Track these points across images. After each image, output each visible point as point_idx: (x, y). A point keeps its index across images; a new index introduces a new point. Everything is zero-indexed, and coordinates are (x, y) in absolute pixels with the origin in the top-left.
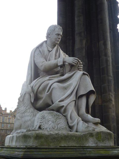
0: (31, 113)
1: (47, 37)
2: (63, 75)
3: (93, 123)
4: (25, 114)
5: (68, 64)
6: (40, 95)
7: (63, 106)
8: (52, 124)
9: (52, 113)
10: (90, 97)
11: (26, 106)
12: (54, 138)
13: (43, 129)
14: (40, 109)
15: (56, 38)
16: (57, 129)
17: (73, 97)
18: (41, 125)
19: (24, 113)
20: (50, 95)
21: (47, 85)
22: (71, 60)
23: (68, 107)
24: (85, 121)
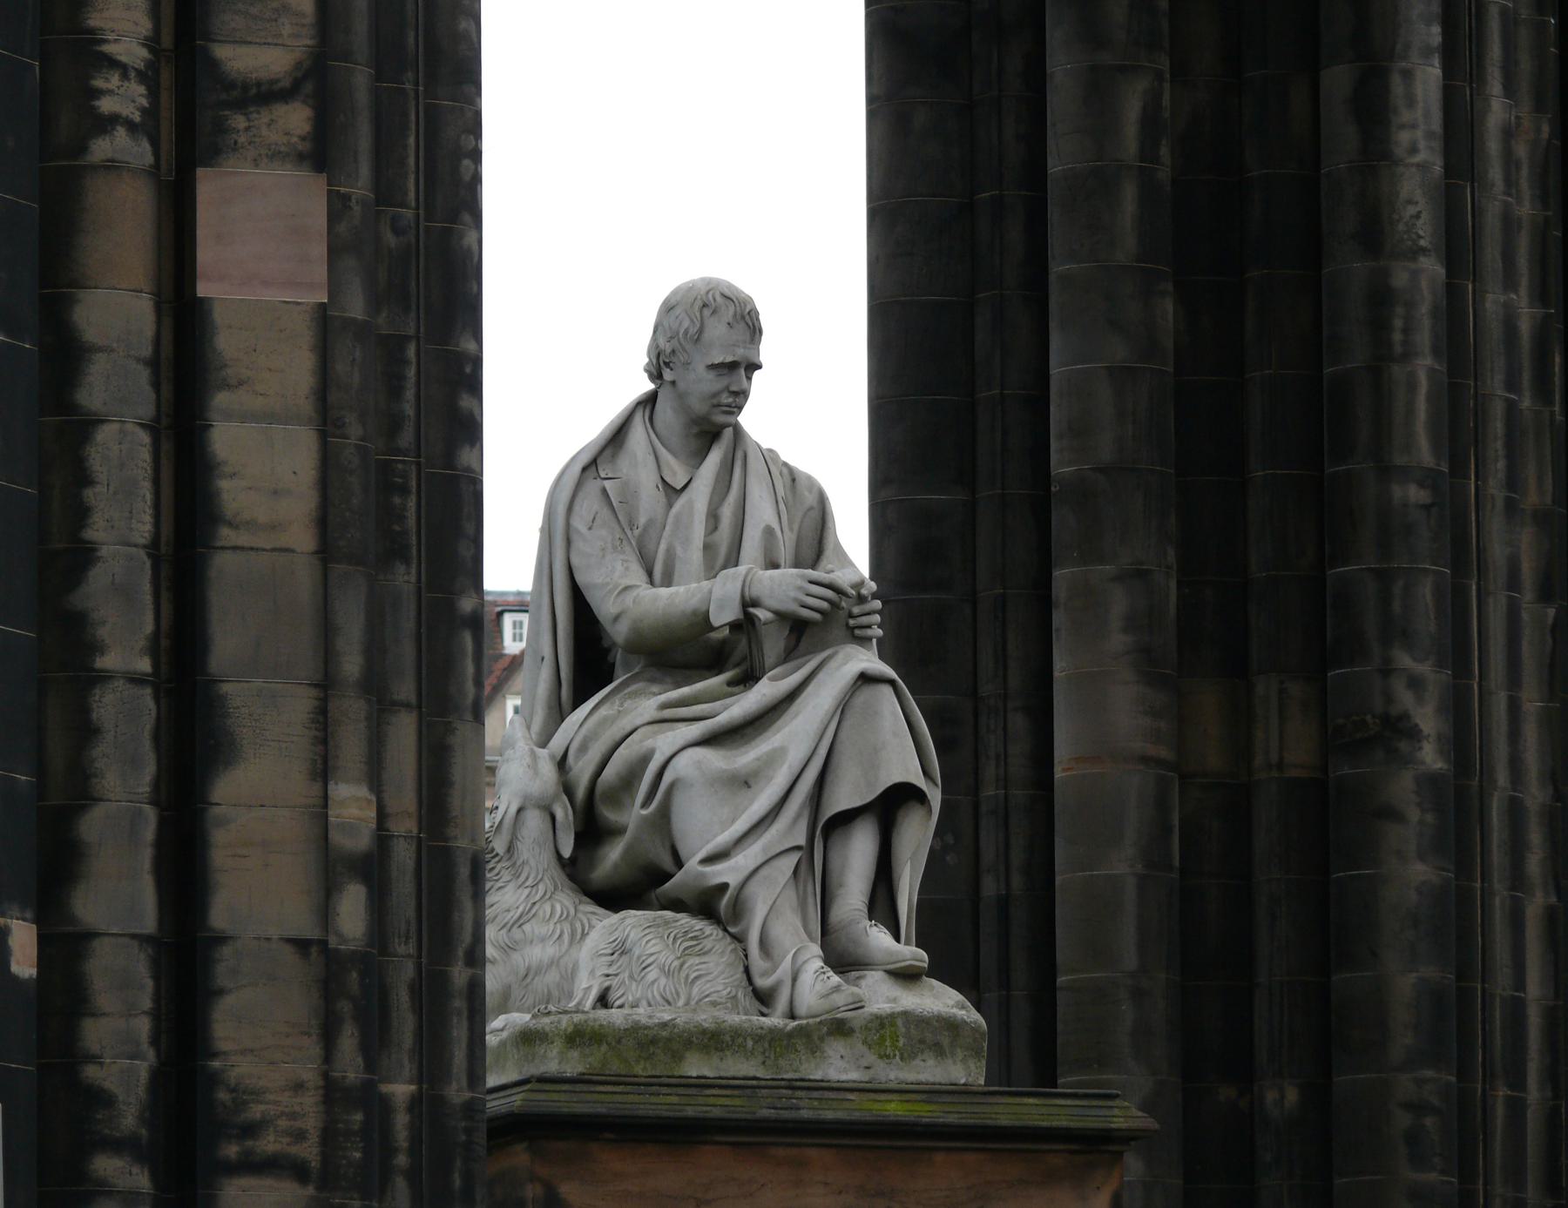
0: (559, 921)
1: (656, 373)
2: (748, 679)
3: (890, 973)
4: (527, 927)
5: (769, 615)
6: (610, 815)
7: (724, 887)
8: (663, 981)
9: (667, 923)
10: (900, 819)
11: (529, 883)
12: (654, 1041)
13: (621, 1007)
14: (613, 898)
15: (716, 395)
16: (687, 1004)
17: (790, 830)
18: (608, 989)
19: (519, 922)
20: (663, 820)
21: (645, 759)
22: (793, 594)
23: (753, 888)
24: (843, 960)
